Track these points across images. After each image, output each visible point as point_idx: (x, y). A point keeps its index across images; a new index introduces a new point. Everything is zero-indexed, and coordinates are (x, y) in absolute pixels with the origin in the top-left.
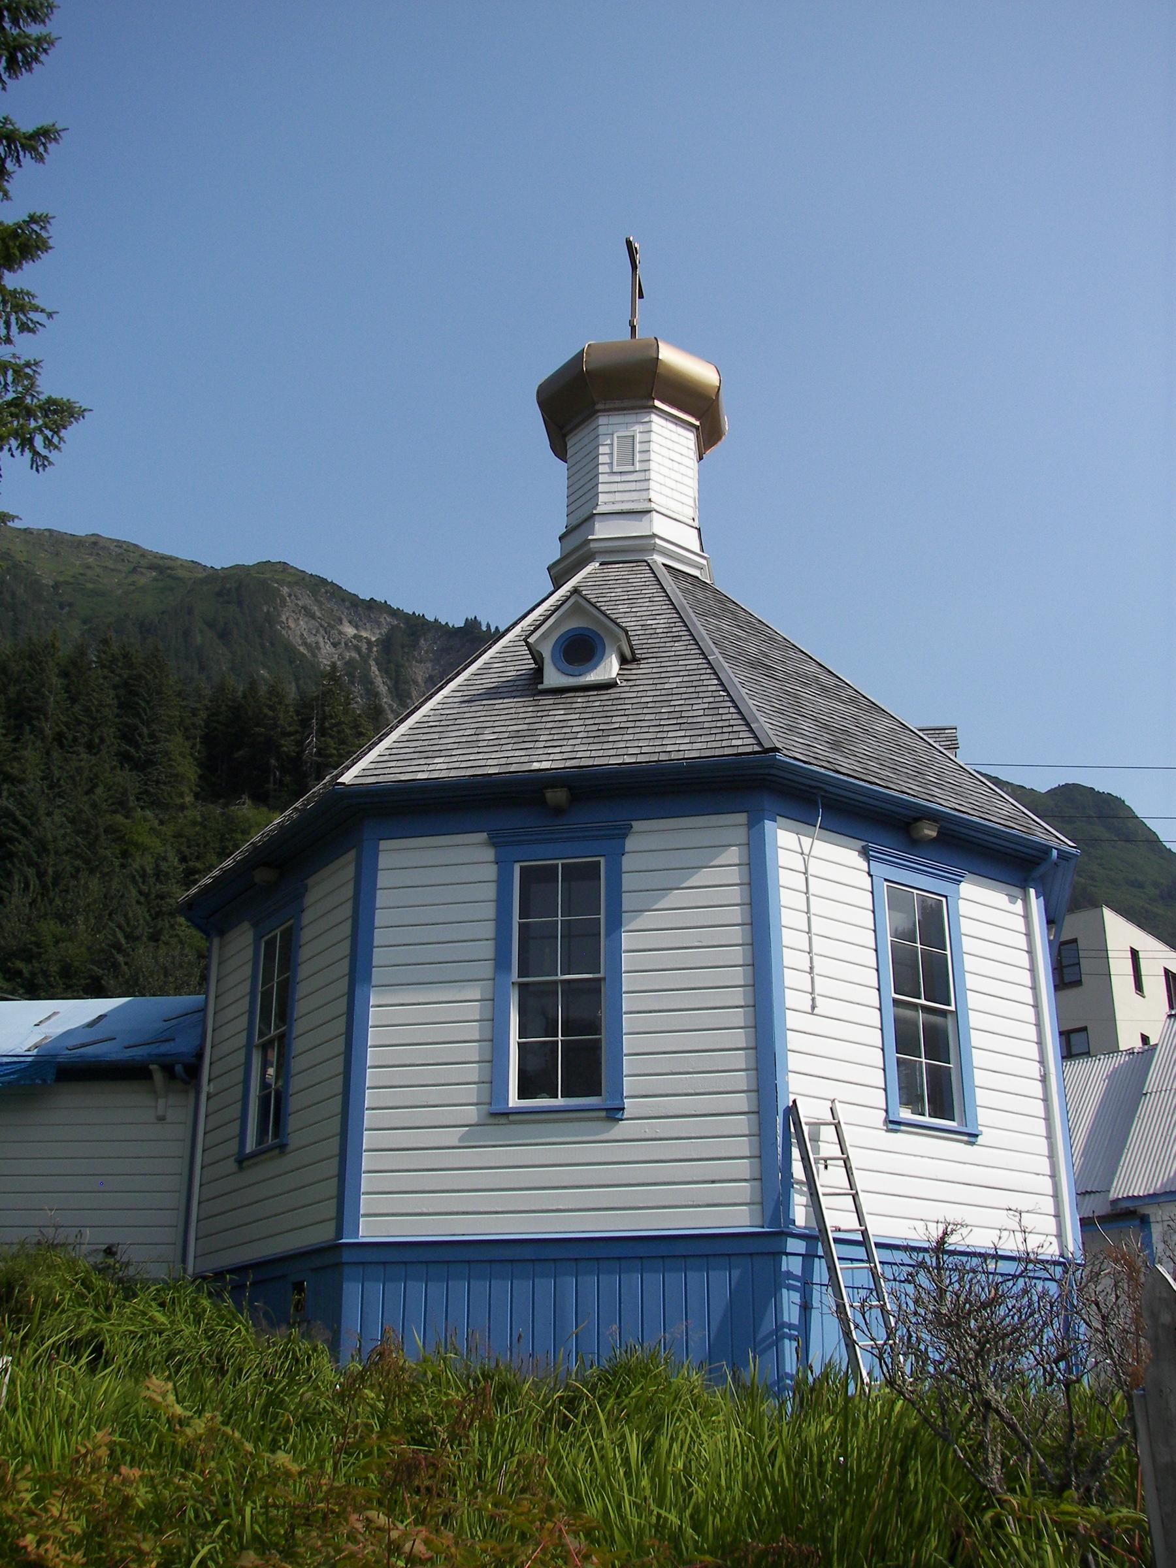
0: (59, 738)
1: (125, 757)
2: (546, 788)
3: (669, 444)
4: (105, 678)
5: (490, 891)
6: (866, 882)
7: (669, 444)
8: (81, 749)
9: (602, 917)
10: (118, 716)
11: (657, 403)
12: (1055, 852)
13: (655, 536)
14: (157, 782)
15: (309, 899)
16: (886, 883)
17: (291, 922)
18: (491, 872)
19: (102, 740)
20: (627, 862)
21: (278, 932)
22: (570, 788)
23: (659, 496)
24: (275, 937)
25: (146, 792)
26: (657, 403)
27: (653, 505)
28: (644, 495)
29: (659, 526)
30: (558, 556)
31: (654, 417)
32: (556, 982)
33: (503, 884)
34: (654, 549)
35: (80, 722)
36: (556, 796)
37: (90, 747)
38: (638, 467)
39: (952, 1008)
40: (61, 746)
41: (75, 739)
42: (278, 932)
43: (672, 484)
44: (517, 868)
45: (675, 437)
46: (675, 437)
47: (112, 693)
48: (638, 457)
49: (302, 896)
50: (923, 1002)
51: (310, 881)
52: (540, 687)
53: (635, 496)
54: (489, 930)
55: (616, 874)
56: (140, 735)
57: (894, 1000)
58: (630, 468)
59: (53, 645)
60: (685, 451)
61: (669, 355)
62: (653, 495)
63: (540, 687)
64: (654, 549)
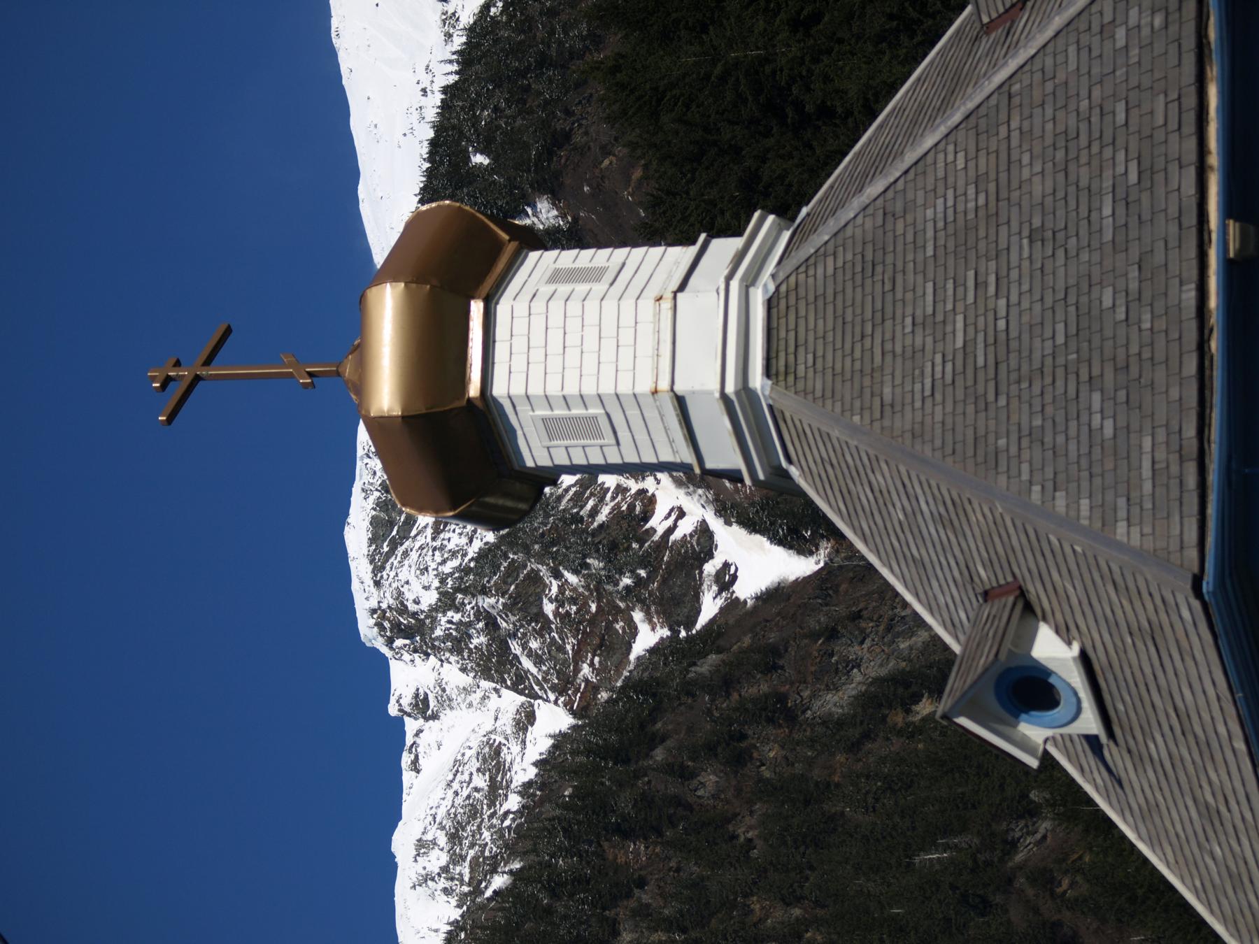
0: (800, 25)
3: (536, 355)
7: (536, 355)
11: (474, 390)
13: (724, 396)
23: (642, 376)
26: (474, 390)
27: (664, 385)
28: (647, 402)
29: (702, 376)
31: (499, 390)
34: (745, 388)
38: (595, 410)
40: (816, 17)
45: (520, 344)
46: (520, 344)
48: (577, 411)
53: (652, 415)
58: (604, 422)
59: (616, 69)
61: (386, 393)
62: (644, 387)
64: (745, 388)
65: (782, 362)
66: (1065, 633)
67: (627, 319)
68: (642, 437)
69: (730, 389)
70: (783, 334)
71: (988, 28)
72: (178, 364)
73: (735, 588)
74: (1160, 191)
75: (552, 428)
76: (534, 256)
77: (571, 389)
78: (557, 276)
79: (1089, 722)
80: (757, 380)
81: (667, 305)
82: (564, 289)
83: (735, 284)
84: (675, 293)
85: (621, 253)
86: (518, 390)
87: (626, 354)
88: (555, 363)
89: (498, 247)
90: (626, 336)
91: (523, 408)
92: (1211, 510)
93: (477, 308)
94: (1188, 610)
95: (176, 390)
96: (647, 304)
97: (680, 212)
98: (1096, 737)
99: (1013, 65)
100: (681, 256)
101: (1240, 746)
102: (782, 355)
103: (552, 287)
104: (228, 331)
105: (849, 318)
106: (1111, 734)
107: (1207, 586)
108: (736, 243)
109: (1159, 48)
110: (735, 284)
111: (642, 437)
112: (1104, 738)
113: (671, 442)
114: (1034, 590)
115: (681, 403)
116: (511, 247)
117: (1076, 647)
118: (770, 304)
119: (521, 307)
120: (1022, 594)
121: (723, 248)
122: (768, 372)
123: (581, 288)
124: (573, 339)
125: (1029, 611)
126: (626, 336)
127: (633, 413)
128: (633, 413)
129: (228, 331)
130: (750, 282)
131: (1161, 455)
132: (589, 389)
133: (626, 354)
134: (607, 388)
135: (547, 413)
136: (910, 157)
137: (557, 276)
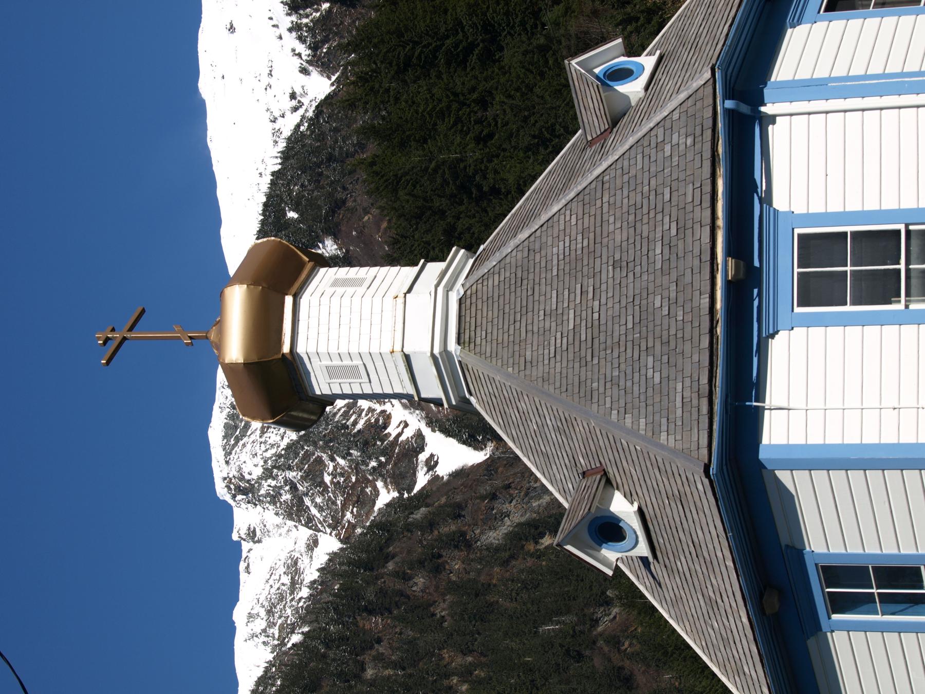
0: (482, 140)
1: (488, 58)
4: (397, 99)
6: (799, 332)
8: (490, 113)
10: (439, 77)
11: (286, 349)
13: (433, 356)
14: (507, 14)
19: (473, 89)
22: (761, 596)
25: (523, 24)
26: (286, 349)
27: (398, 348)
28: (387, 357)
29: (420, 345)
34: (445, 351)
35: (459, 120)
37: (483, 103)
39: (902, 227)
40: (491, 136)
41: (479, 122)
43: (366, 324)
45: (314, 322)
46: (314, 322)
47: (413, 88)
48: (347, 362)
50: (902, 266)
53: (390, 366)
54: (892, 638)
56: (456, 46)
59: (373, 164)
61: (235, 349)
62: (386, 349)
64: (445, 351)
65: (467, 336)
66: (629, 497)
67: (377, 309)
68: (384, 378)
69: (436, 351)
70: (468, 319)
71: (590, 143)
72: (113, 330)
73: (437, 469)
74: (689, 240)
75: (332, 372)
76: (323, 271)
77: (343, 350)
78: (336, 283)
79: (643, 549)
80: (452, 346)
81: (400, 300)
82: (340, 290)
83: (440, 289)
84: (405, 294)
85: (374, 270)
86: (312, 350)
87: (376, 329)
88: (334, 334)
89: (302, 265)
90: (376, 319)
91: (315, 360)
92: (716, 427)
93: (289, 300)
94: (702, 484)
95: (112, 346)
96: (389, 299)
97: (410, 246)
98: (647, 558)
99: (605, 165)
100: (409, 272)
101: (730, 564)
102: (467, 331)
103: (333, 289)
104: (143, 311)
105: (507, 310)
106: (655, 556)
107: (713, 470)
108: (441, 265)
109: (690, 156)
110: (440, 289)
111: (384, 378)
112: (651, 559)
113: (401, 382)
114: (612, 471)
115: (407, 358)
116: (310, 265)
117: (636, 505)
118: (461, 302)
119: (315, 300)
120: (605, 473)
121: (434, 268)
122: (459, 343)
123: (350, 290)
124: (345, 320)
125: (609, 483)
126: (376, 319)
127: (379, 364)
128: (379, 364)
129: (143, 311)
130: (449, 288)
131: (687, 394)
132: (354, 350)
133: (376, 329)
134: (364, 350)
135: (329, 363)
136: (544, 217)
137: (336, 283)
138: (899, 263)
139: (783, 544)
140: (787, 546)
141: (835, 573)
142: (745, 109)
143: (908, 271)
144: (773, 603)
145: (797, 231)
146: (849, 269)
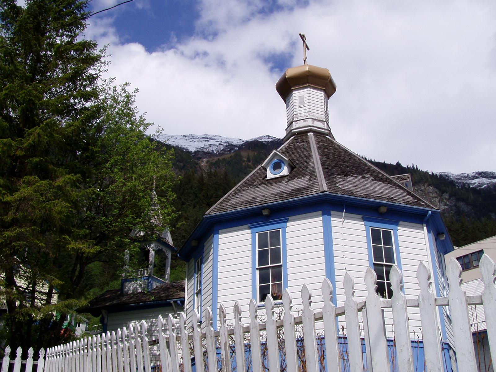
2: (262, 210)
5: (250, 242)
6: (364, 228)
9: (281, 246)
12: (430, 212)
15: (205, 250)
16: (370, 228)
17: (201, 257)
18: (250, 236)
20: (287, 229)
21: (199, 259)
22: (270, 209)
24: (199, 261)
30: (285, 135)
32: (269, 267)
33: (253, 239)
36: (265, 212)
42: (199, 259)
44: (257, 234)
49: (203, 248)
50: (384, 263)
51: (205, 244)
52: (266, 179)
54: (250, 253)
55: (284, 233)
57: (374, 264)
60: (321, 98)
63: (266, 179)
73: (203, 147)
79: (270, 175)
104: (308, 49)
138: (385, 262)
139: (289, 217)
140: (288, 219)
141: (276, 236)
142: (426, 219)
143: (382, 265)
144: (265, 212)
145: (392, 231)
146: (383, 246)
